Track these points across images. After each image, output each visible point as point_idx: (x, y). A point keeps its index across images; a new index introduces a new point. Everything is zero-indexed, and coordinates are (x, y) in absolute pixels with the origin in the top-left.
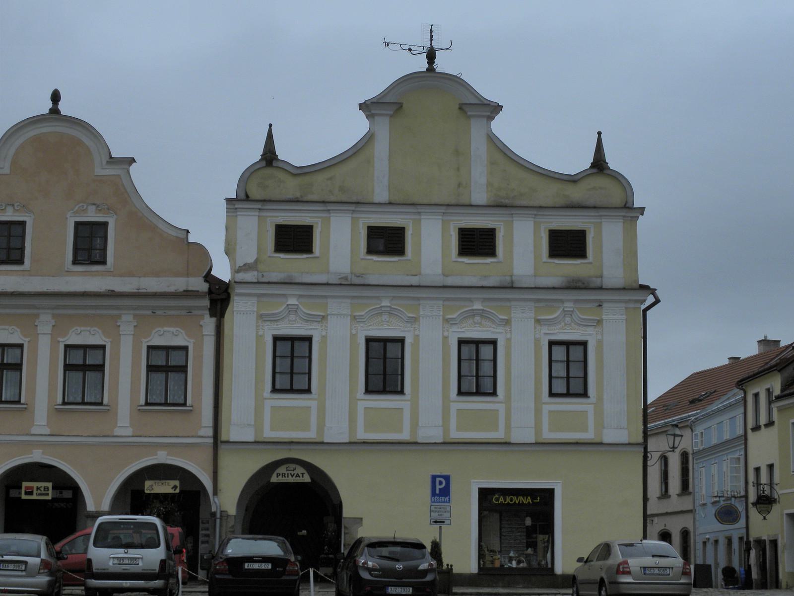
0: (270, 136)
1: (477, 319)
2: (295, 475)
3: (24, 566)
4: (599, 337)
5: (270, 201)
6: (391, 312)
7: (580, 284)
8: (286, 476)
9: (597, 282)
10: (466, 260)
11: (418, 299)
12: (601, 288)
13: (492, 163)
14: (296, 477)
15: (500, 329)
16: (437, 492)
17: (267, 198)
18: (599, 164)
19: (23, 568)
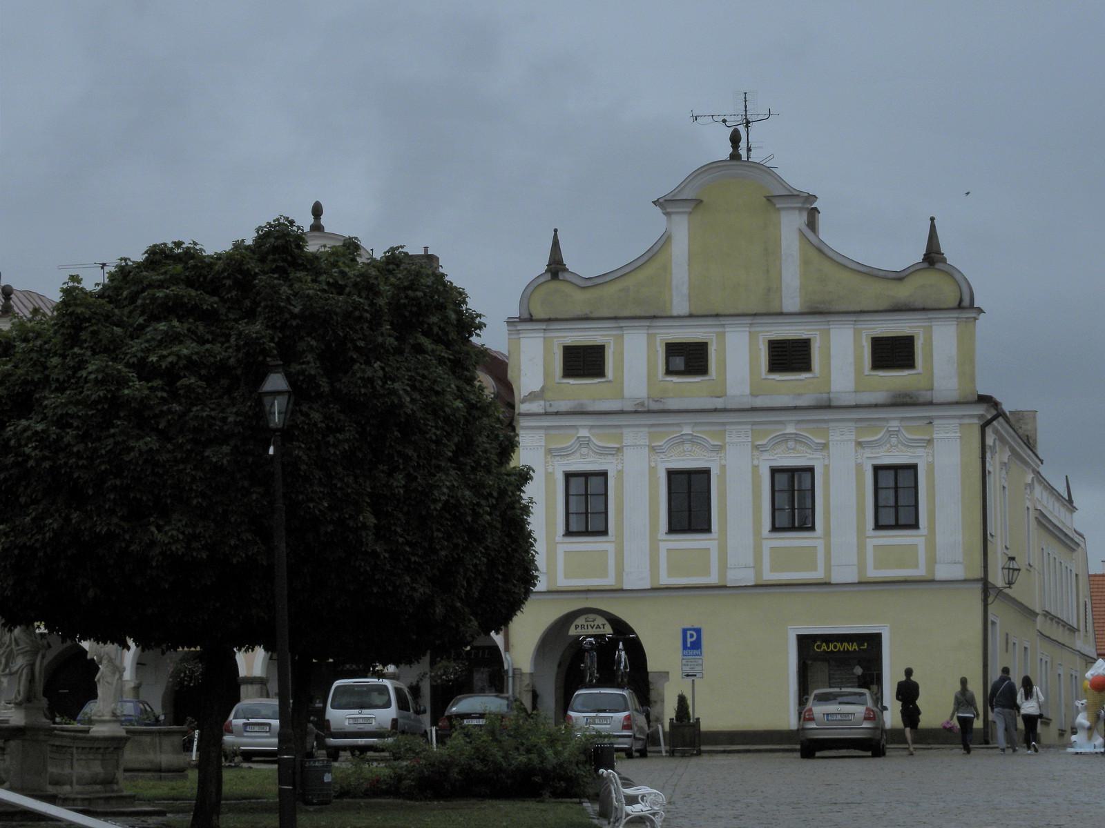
0: (556, 244)
1: (791, 444)
2: (595, 628)
3: (268, 728)
4: (930, 459)
5: (557, 320)
6: (693, 440)
7: (908, 400)
8: (586, 627)
9: (926, 396)
10: (778, 377)
11: (724, 424)
12: (931, 404)
13: (806, 262)
14: (597, 628)
15: (818, 455)
16: (689, 645)
17: (552, 316)
18: (933, 256)
19: (268, 730)
